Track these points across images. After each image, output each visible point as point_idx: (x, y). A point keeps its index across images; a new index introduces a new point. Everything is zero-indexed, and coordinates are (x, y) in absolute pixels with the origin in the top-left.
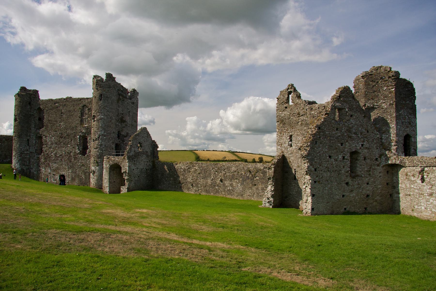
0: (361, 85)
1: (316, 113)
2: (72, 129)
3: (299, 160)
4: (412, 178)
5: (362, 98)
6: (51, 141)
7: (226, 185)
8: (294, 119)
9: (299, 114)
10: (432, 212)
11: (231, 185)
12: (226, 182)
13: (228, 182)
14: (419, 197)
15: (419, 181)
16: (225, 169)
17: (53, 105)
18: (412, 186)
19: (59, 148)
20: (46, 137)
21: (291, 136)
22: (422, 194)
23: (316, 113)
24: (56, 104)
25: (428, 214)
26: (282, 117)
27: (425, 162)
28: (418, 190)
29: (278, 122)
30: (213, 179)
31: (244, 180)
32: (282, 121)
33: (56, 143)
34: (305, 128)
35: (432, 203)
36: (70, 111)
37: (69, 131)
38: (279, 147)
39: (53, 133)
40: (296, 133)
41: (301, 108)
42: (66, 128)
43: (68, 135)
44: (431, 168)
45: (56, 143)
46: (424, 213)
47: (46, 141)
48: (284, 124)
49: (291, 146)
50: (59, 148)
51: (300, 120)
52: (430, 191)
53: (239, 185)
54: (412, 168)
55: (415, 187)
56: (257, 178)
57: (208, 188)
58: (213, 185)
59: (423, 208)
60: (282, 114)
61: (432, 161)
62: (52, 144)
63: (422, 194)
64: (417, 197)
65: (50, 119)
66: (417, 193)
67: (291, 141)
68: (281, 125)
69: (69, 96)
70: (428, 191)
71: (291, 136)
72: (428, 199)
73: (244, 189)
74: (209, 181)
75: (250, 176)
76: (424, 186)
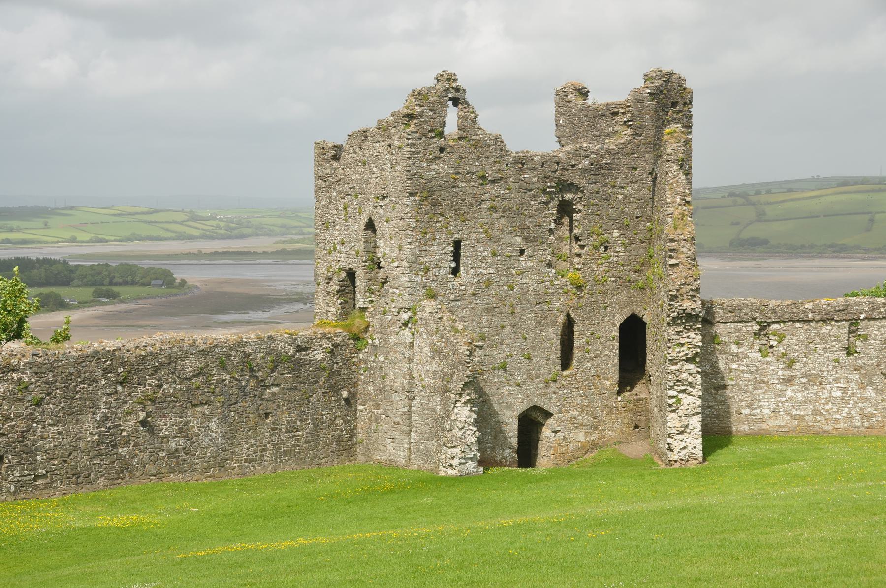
0: (647, 116)
1: (535, 180)
3: (485, 318)
4: (734, 349)
5: (648, 152)
7: (164, 433)
8: (470, 191)
9: (483, 177)
10: (793, 418)
11: (183, 431)
12: (161, 422)
13: (171, 419)
14: (755, 389)
15: (755, 355)
16: (156, 370)
18: (735, 366)
21: (457, 244)
22: (763, 382)
23: (535, 180)
25: (783, 423)
26: (429, 181)
27: (775, 312)
28: (751, 372)
29: (411, 194)
30: (105, 418)
31: (229, 405)
32: (431, 191)
34: (502, 221)
35: (791, 398)
38: (419, 279)
40: (473, 236)
41: (492, 160)
44: (790, 324)
46: (771, 423)
48: (435, 204)
49: (455, 272)
51: (486, 196)
52: (787, 373)
53: (213, 426)
54: (733, 325)
55: (741, 368)
56: (275, 389)
57: (83, 460)
58: (109, 440)
59: (766, 411)
60: (429, 170)
61: (795, 310)
63: (763, 382)
64: (750, 388)
66: (749, 381)
67: (456, 256)
68: (426, 207)
70: (780, 373)
71: (457, 244)
72: (781, 391)
73: (230, 437)
74: (89, 428)
75: (253, 382)
76: (768, 363)
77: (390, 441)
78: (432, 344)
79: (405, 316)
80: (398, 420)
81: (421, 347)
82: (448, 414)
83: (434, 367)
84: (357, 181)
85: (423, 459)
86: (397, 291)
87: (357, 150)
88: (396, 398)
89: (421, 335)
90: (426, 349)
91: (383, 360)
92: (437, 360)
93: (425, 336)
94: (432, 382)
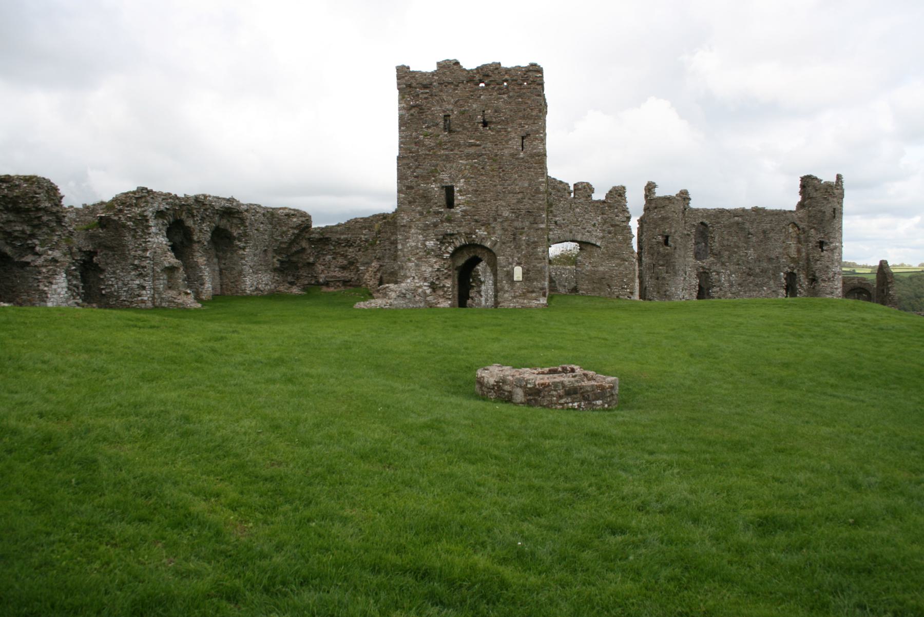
2: (770, 260)
6: (729, 281)
17: (732, 220)
19: (745, 292)
20: (718, 273)
24: (736, 218)
33: (739, 284)
36: (764, 232)
37: (765, 265)
39: (732, 268)
42: (758, 260)
43: (764, 271)
45: (739, 284)
47: (720, 281)
50: (745, 292)
62: (731, 286)
65: (725, 243)
69: (760, 206)
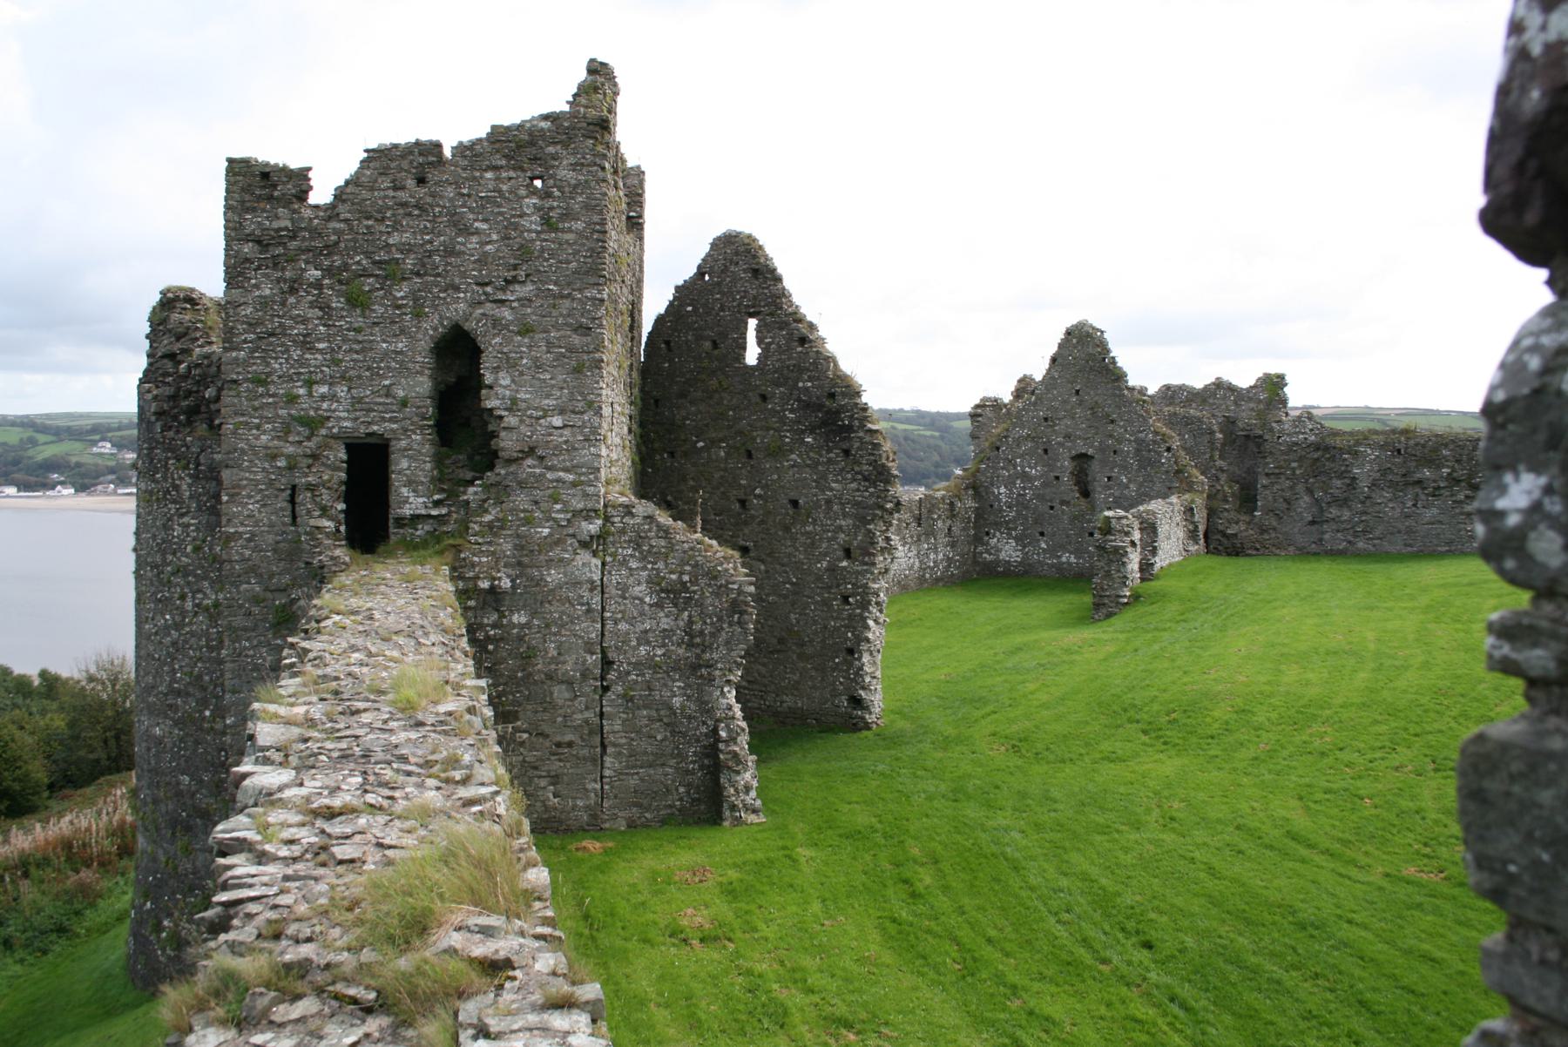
77: (543, 783)
78: (654, 582)
79: (594, 527)
80: (568, 737)
81: (623, 588)
82: (706, 708)
83: (666, 623)
84: (407, 249)
85: (636, 805)
86: (571, 477)
87: (411, 183)
88: (560, 693)
89: (624, 563)
90: (639, 590)
91: (523, 620)
92: (669, 608)
93: (634, 565)
94: (659, 652)
